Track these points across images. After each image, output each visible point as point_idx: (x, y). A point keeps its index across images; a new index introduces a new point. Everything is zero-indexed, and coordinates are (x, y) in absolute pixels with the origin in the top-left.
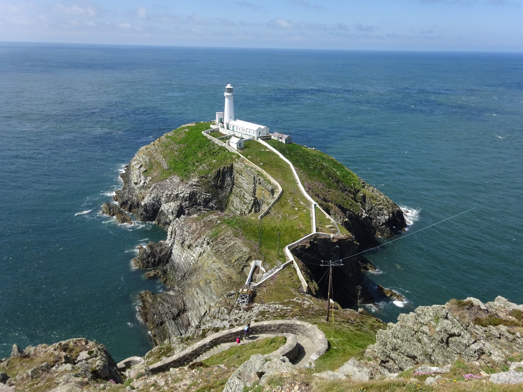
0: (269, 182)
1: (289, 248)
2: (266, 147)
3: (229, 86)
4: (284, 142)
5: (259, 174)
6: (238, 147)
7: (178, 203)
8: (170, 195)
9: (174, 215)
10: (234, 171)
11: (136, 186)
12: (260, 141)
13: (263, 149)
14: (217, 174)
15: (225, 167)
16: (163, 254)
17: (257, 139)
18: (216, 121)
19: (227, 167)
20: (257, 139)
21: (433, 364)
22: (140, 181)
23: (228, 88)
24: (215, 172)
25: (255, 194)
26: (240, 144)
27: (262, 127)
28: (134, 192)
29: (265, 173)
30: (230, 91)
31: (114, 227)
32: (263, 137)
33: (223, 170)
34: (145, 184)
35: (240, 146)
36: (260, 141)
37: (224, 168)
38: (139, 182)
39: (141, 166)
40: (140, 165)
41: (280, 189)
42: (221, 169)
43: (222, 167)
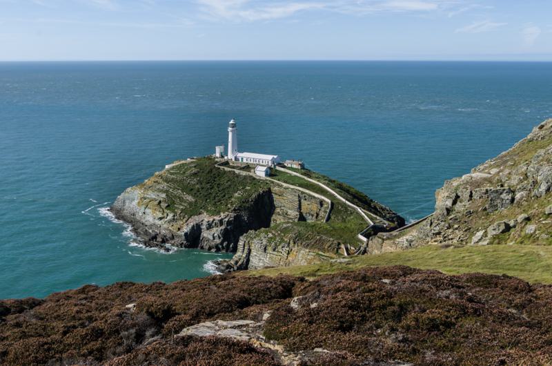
0: (314, 197)
1: (361, 235)
3: (232, 122)
5: (303, 193)
7: (223, 227)
8: (213, 222)
9: (222, 239)
21: (512, 189)
25: (300, 210)
27: (275, 157)
29: (307, 191)
30: (234, 125)
31: (162, 255)
37: (264, 192)
39: (160, 202)
41: (329, 201)
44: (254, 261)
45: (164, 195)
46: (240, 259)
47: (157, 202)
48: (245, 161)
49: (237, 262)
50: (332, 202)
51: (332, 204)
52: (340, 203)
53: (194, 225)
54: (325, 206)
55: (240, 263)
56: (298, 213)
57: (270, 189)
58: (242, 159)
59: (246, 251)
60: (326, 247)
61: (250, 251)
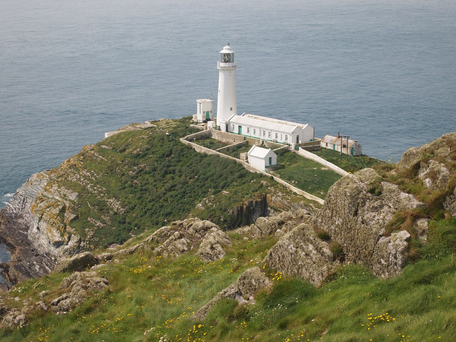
2: (318, 164)
3: (225, 50)
4: (349, 153)
6: (268, 165)
10: (269, 209)
11: (58, 249)
12: (302, 152)
13: (315, 167)
14: (238, 215)
15: (252, 202)
17: (297, 149)
18: (196, 117)
19: (256, 202)
20: (297, 149)
22: (69, 238)
23: (225, 55)
24: (233, 213)
26: (270, 158)
28: (56, 260)
30: (228, 58)
32: (306, 144)
33: (248, 208)
34: (82, 244)
35: (270, 162)
36: (302, 152)
38: (67, 240)
40: (61, 207)
42: (245, 207)
43: (246, 203)
47: (56, 211)
48: (244, 132)
57: (265, 198)
58: (240, 127)
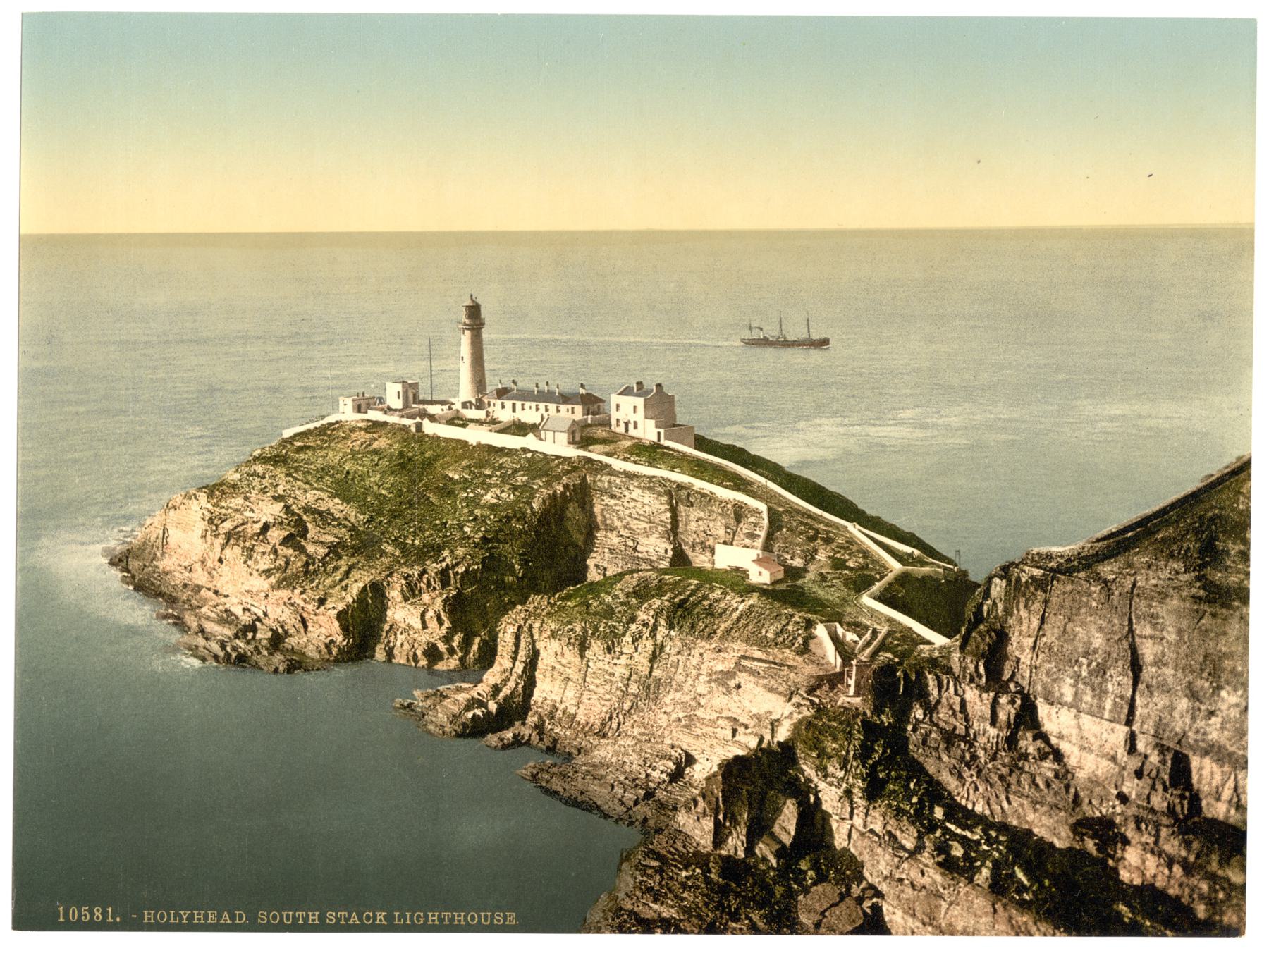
16: (502, 695)
25: (675, 535)
33: (563, 494)
34: (311, 568)
40: (260, 525)
41: (762, 507)
44: (545, 691)
45: (277, 508)
46: (506, 680)
49: (496, 689)
50: (769, 509)
51: (772, 514)
52: (794, 511)
53: (365, 586)
54: (752, 519)
55: (505, 691)
56: (670, 547)
59: (522, 654)
60: (770, 635)
61: (534, 656)
